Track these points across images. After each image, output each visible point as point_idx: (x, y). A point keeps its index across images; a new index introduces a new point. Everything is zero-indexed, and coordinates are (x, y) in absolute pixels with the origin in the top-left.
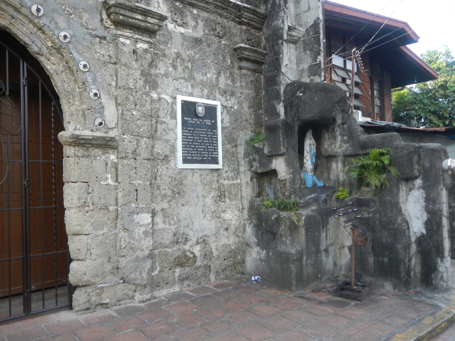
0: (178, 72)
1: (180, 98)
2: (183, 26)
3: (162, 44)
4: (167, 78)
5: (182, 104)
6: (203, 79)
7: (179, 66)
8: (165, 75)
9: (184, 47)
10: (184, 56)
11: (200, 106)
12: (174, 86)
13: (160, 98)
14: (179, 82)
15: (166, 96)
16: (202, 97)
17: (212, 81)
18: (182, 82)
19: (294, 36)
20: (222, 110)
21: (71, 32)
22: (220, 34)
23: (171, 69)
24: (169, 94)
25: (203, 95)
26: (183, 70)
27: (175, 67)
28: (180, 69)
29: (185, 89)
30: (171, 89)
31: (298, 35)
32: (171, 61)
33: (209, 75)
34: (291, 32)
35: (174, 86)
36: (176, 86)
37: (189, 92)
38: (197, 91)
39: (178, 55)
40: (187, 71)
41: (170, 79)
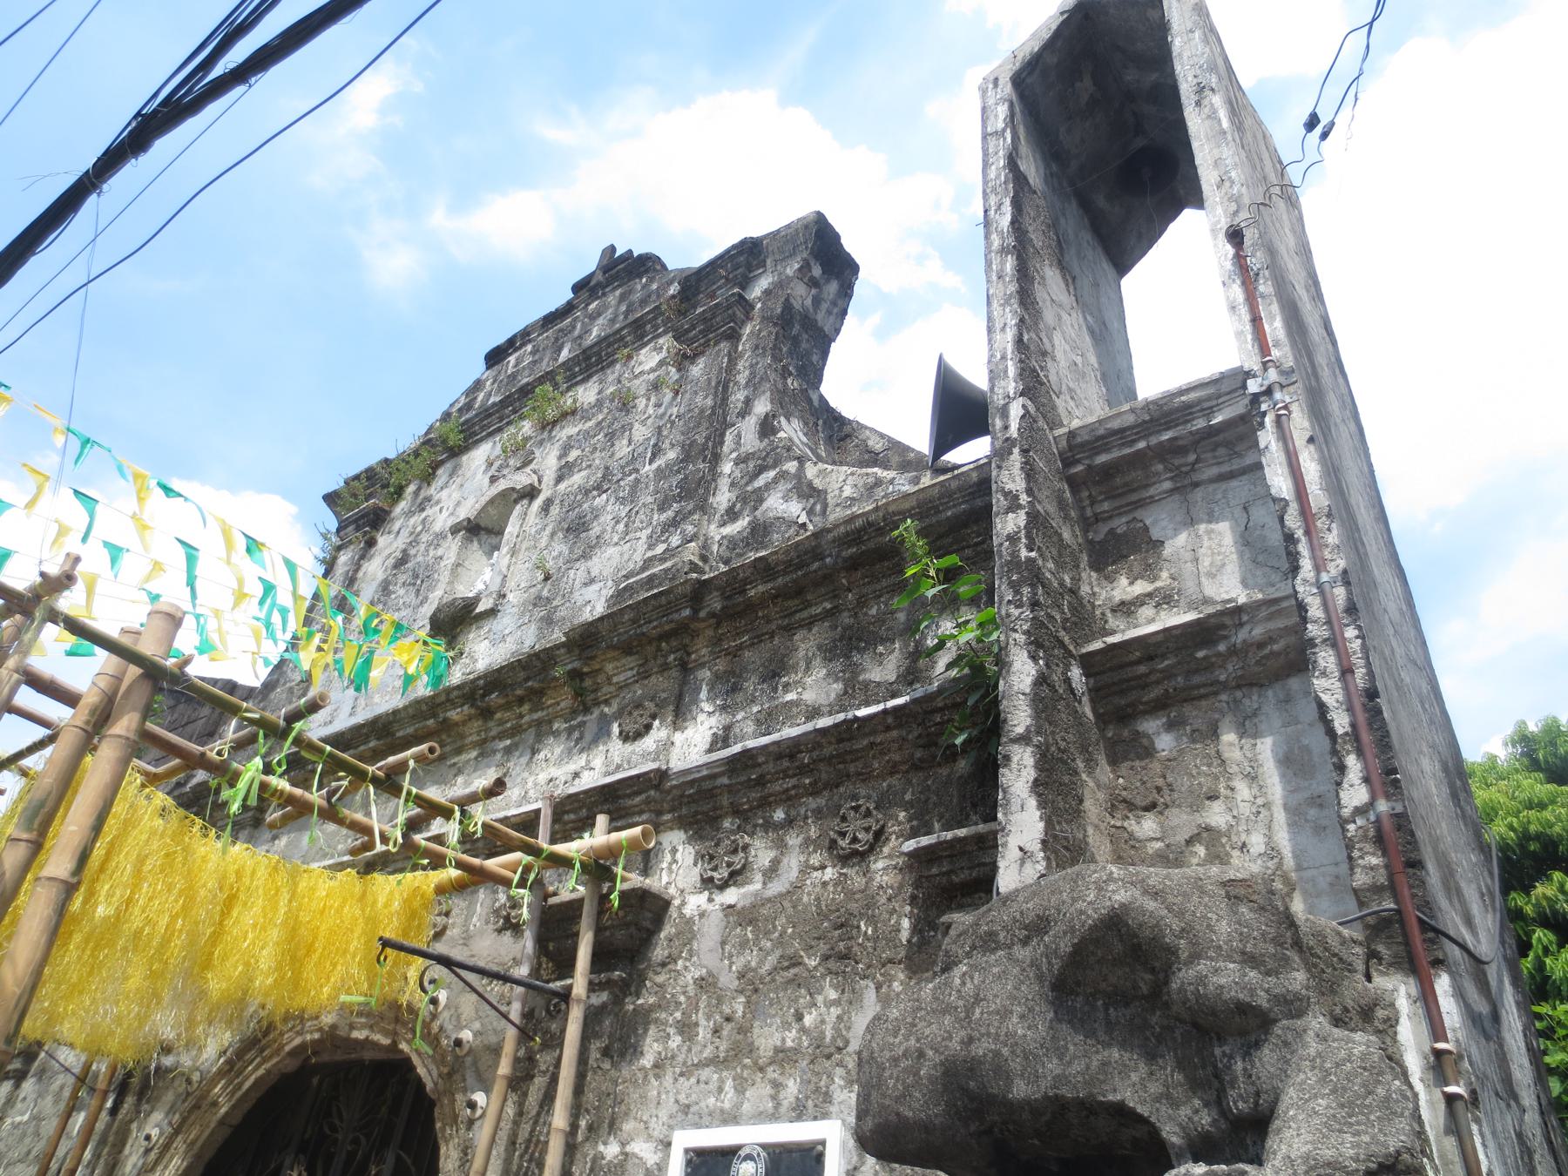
0: (698, 1042)
1: (689, 1138)
2: (735, 884)
3: (659, 969)
4: (657, 1077)
5: (689, 1163)
6: (783, 1040)
7: (703, 1022)
8: (656, 1066)
9: (727, 948)
10: (728, 980)
11: (749, 1157)
12: (677, 1101)
13: (626, 1154)
14: (693, 1080)
15: (645, 1146)
16: (774, 1117)
17: (822, 1033)
18: (703, 1078)
19: (1261, 645)
20: (855, 1158)
21: (477, 1025)
22: (860, 841)
23: (675, 1041)
24: (656, 1134)
25: (778, 1105)
26: (716, 1031)
27: (687, 1029)
28: (703, 1033)
29: (712, 1100)
30: (663, 1114)
31: (1280, 623)
32: (678, 1015)
33: (808, 1020)
34: (1226, 637)
35: (677, 1101)
36: (682, 1098)
37: (722, 1111)
38: (758, 1094)
39: (706, 984)
40: (727, 1029)
41: (668, 1079)
